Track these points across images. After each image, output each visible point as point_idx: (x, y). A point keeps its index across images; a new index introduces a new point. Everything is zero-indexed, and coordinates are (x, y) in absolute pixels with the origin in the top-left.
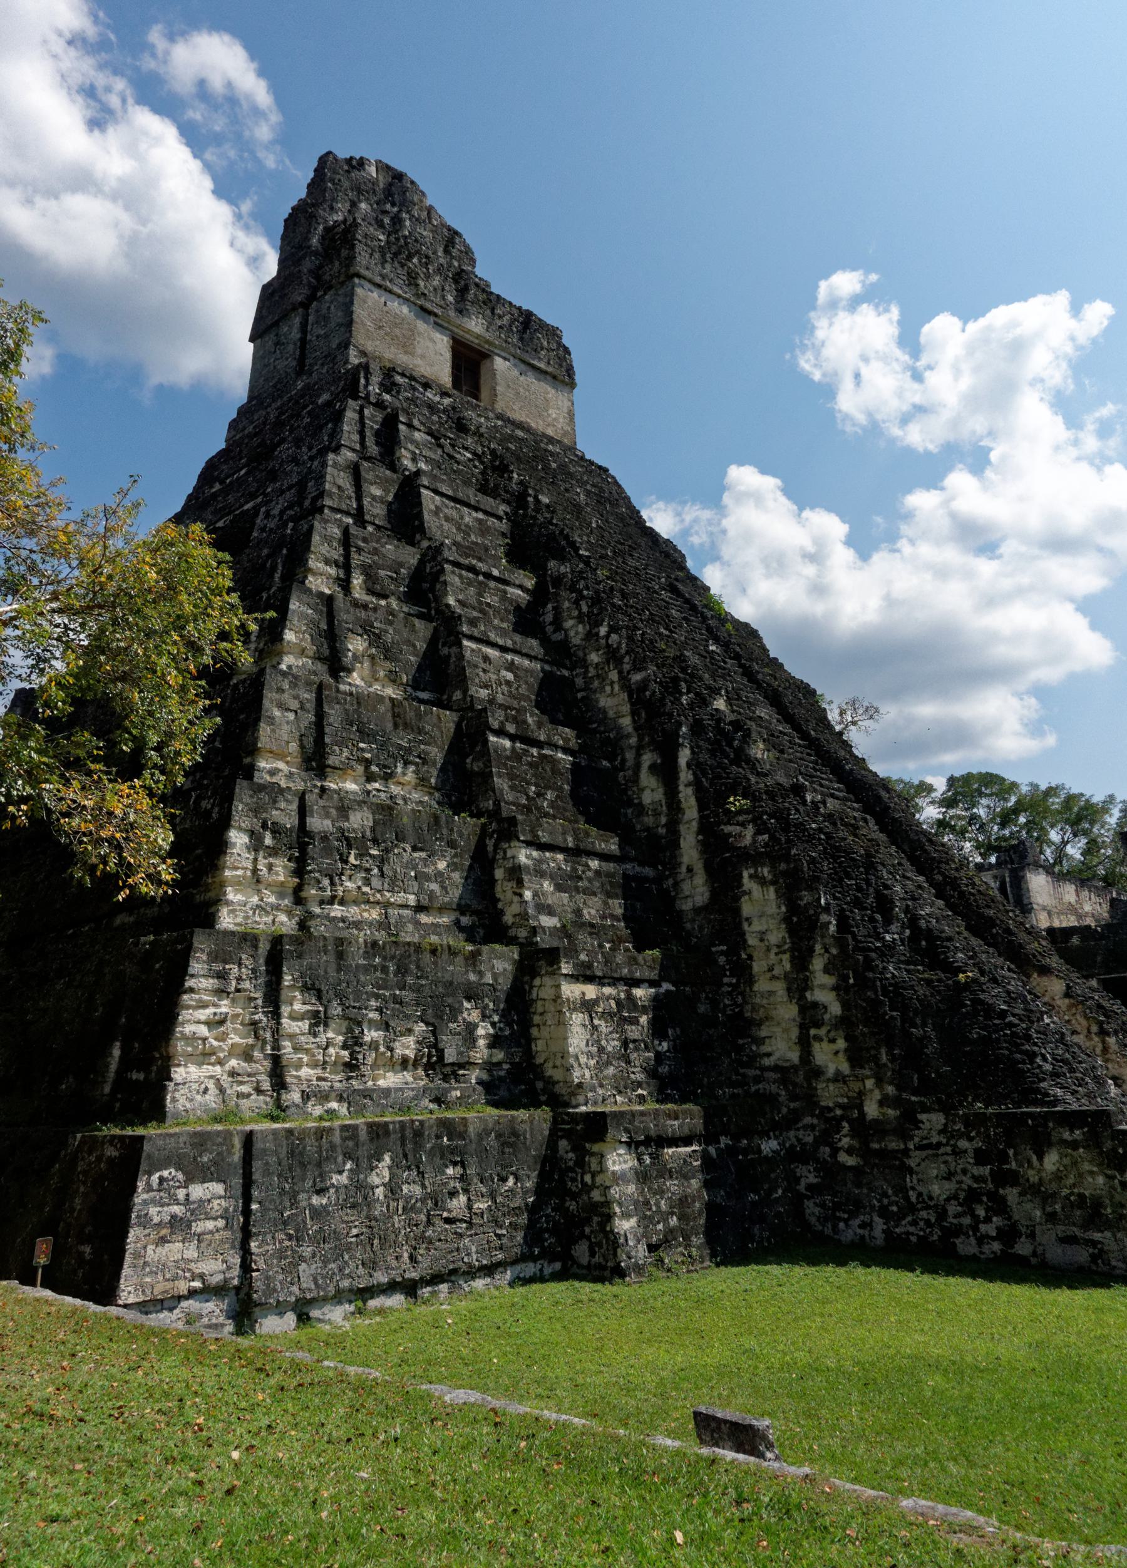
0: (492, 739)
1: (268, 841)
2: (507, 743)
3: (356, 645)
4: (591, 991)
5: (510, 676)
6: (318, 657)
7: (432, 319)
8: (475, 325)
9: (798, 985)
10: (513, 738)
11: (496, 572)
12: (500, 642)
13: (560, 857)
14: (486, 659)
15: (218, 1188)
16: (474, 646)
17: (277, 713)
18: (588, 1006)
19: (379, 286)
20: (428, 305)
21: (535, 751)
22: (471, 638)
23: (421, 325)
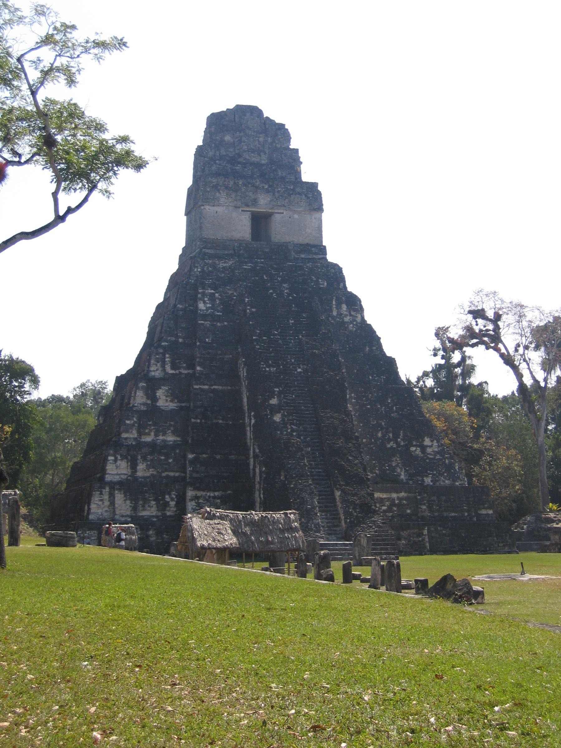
0: (193, 420)
1: (119, 457)
2: (199, 421)
3: (160, 393)
4: (199, 493)
5: (212, 395)
6: (148, 399)
7: (240, 209)
8: (264, 202)
9: (260, 494)
10: (201, 420)
11: (219, 352)
12: (209, 384)
13: (204, 456)
14: (203, 390)
15: (95, 532)
16: (197, 387)
17: (128, 422)
18: (197, 498)
19: (214, 206)
20: (238, 205)
21: (209, 422)
22: (197, 385)
23: (234, 214)
